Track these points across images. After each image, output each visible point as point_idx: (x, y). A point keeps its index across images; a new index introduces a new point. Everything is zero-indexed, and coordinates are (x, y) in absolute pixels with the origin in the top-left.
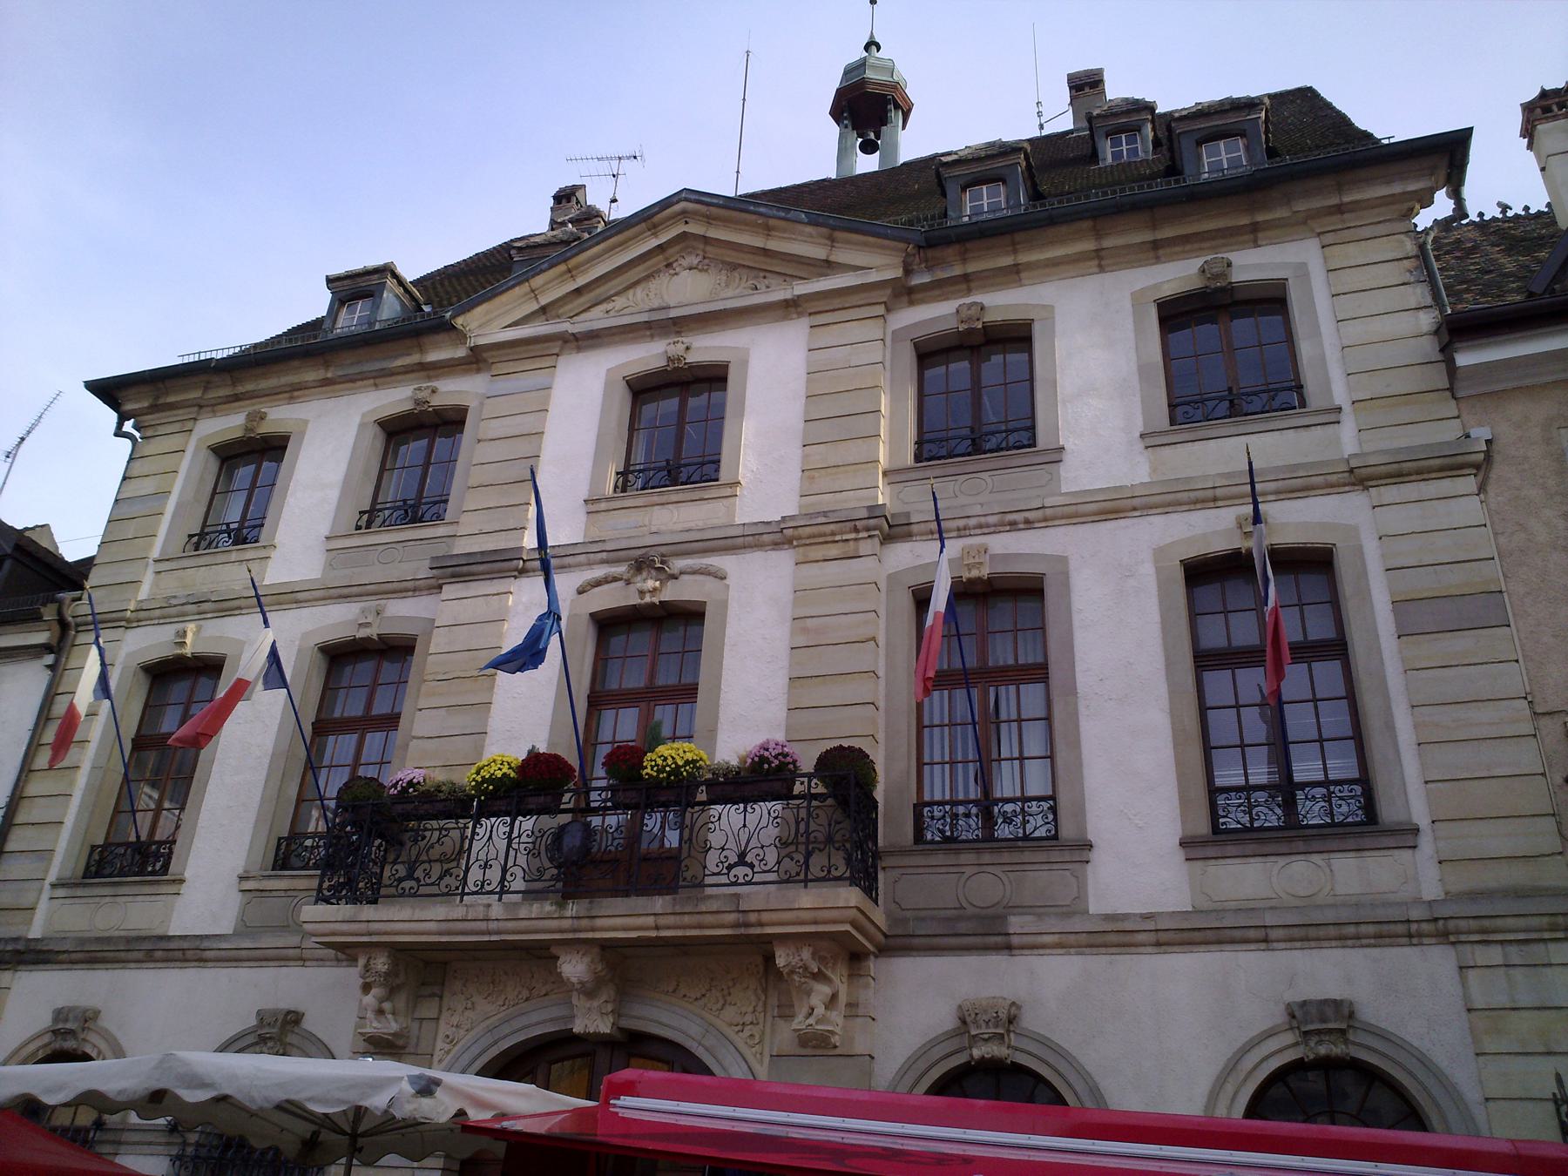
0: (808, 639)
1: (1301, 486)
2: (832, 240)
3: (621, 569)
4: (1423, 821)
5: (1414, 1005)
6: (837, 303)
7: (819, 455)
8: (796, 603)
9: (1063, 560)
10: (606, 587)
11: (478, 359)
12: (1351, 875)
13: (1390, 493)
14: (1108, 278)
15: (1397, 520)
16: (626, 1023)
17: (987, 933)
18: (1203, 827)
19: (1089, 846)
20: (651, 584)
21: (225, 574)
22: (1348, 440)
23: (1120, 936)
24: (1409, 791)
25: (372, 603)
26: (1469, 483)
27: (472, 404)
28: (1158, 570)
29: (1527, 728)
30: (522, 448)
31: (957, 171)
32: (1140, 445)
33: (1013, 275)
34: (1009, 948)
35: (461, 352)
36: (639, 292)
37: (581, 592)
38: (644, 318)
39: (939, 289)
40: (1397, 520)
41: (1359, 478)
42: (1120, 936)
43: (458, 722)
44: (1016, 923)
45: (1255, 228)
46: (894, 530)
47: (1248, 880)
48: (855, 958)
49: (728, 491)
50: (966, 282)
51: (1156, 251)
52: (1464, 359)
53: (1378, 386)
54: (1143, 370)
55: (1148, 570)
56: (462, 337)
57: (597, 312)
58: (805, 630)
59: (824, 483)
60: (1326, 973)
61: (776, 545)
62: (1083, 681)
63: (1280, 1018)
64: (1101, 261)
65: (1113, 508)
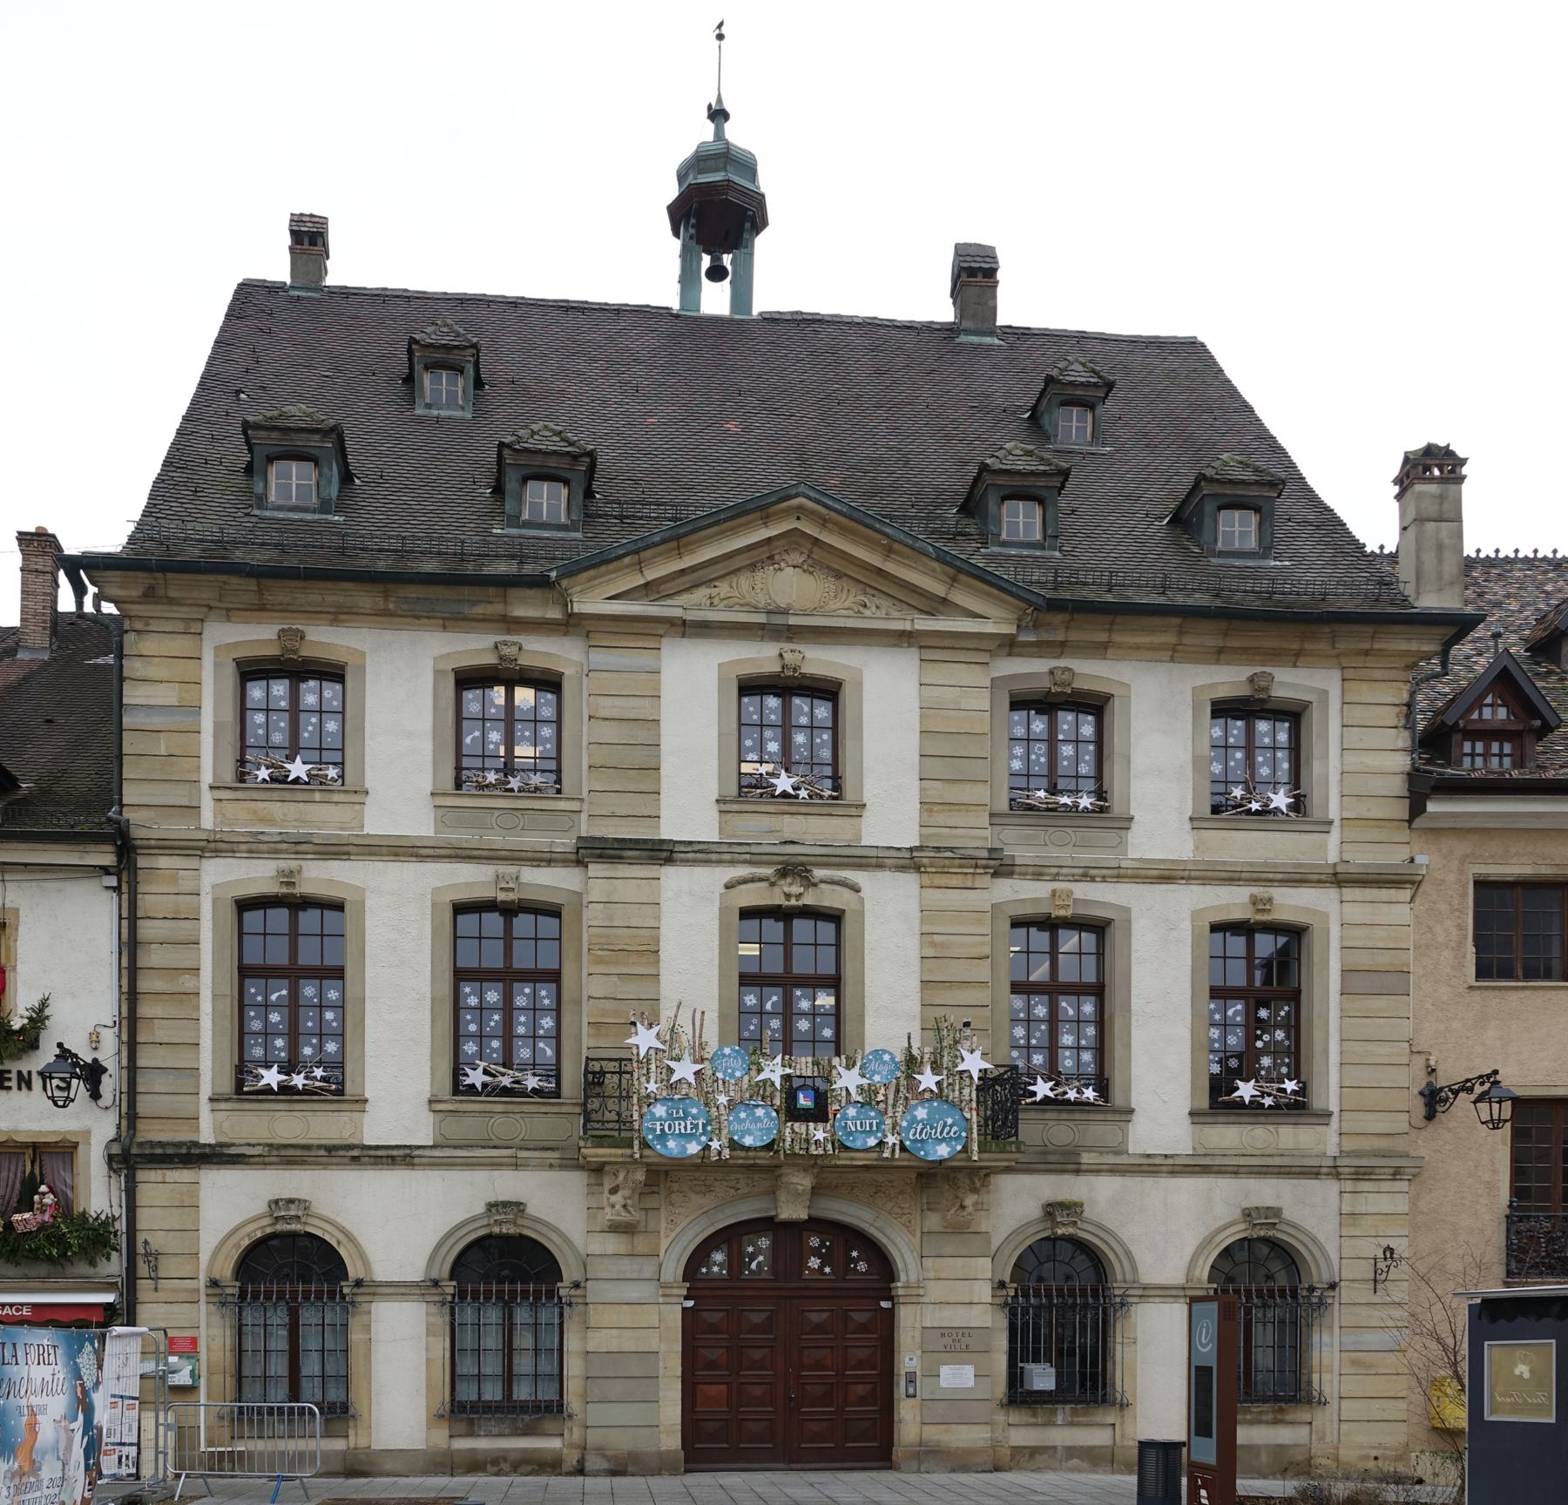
0: (934, 952)
1: (1298, 879)
3: (768, 871)
4: (1334, 1106)
5: (1312, 1213)
11: (572, 624)
12: (1290, 1137)
15: (1355, 913)
17: (1066, 1162)
18: (1204, 1103)
19: (1132, 1111)
22: (1331, 848)
24: (1329, 1091)
25: (511, 869)
26: (1406, 894)
27: (569, 672)
29: (1405, 1060)
30: (641, 735)
32: (1188, 826)
33: (1100, 650)
34: (1077, 1172)
35: (554, 613)
40: (1355, 913)
41: (1338, 879)
43: (629, 990)
44: (1087, 1158)
45: (1298, 654)
46: (1001, 867)
47: (1229, 1136)
49: (853, 811)
50: (1062, 648)
51: (1219, 655)
53: (1363, 809)
55: (1187, 925)
57: (701, 594)
58: (933, 945)
59: (941, 818)
60: (1265, 1192)
61: (901, 868)
62: (1136, 1003)
63: (1237, 1214)
64: (1175, 654)
65: (1167, 875)
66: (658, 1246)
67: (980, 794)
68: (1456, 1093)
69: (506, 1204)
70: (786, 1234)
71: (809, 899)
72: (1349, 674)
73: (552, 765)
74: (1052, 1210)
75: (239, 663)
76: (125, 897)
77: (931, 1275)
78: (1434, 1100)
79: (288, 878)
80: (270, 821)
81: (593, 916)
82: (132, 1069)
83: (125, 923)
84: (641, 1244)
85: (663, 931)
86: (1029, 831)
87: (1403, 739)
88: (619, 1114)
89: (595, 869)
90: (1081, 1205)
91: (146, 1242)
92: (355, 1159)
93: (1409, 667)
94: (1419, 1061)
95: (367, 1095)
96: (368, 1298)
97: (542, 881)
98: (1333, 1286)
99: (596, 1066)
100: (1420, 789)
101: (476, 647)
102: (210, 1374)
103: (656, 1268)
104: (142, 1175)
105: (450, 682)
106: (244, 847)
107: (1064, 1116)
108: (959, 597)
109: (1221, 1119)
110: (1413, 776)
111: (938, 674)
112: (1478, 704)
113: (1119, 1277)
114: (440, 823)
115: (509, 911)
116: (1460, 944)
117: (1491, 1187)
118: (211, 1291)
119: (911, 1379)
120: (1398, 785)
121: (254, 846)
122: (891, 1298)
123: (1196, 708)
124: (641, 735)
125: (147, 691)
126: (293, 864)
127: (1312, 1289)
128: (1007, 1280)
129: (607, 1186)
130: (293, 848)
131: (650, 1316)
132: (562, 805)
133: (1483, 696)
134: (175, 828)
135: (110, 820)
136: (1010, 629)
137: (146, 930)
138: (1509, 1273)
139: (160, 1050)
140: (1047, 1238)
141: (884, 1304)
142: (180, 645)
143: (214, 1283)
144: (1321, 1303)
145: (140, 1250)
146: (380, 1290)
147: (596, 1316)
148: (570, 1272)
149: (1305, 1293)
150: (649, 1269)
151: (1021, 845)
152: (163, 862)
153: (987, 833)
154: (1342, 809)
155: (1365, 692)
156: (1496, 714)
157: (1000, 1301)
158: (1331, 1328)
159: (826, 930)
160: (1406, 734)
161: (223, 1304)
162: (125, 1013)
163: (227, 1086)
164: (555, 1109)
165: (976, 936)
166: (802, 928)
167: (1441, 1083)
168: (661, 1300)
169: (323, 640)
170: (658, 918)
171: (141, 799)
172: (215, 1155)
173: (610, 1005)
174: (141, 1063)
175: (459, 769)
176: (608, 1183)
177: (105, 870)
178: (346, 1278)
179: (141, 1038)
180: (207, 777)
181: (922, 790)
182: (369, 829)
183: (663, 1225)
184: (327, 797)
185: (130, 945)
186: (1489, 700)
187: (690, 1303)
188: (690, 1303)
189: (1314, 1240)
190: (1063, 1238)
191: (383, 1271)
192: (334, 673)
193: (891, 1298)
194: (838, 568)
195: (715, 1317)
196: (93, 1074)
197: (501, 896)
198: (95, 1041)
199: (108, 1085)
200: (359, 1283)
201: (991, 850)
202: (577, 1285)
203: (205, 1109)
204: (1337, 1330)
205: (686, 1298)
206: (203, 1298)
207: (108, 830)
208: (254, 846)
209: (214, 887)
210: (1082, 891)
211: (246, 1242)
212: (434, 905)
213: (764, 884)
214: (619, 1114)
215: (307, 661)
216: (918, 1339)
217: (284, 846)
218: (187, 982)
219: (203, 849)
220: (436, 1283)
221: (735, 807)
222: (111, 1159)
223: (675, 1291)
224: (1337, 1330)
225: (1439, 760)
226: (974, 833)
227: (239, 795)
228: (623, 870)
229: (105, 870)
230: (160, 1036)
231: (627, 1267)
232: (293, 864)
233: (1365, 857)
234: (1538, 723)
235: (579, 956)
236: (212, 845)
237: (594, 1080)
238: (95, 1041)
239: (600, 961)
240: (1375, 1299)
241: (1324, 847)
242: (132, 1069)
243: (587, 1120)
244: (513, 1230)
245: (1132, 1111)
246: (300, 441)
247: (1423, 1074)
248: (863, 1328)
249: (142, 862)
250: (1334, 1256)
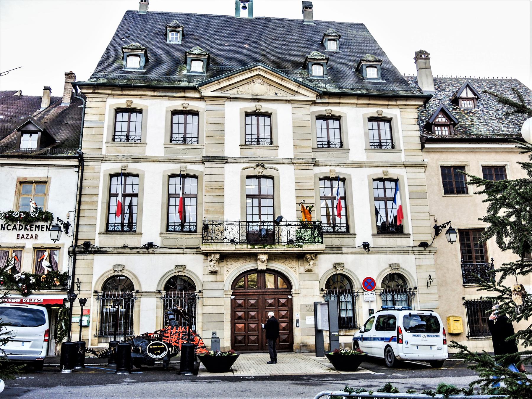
2: (299, 87)
3: (254, 165)
4: (411, 233)
6: (299, 103)
7: (299, 143)
8: (296, 179)
11: (202, 98)
15: (411, 176)
16: (268, 267)
17: (338, 250)
19: (356, 234)
20: (261, 170)
22: (402, 158)
26: (423, 170)
28: (368, 180)
29: (428, 218)
30: (219, 128)
31: (312, 61)
32: (365, 151)
35: (197, 95)
36: (246, 86)
38: (251, 97)
40: (411, 176)
48: (316, 254)
49: (276, 148)
52: (427, 146)
53: (409, 147)
55: (366, 179)
56: (199, 92)
58: (298, 186)
59: (299, 150)
66: (224, 278)
67: (309, 143)
68: (442, 227)
69: (181, 266)
70: (262, 273)
71: (265, 173)
72: (402, 110)
73: (196, 136)
74: (336, 266)
75: (116, 109)
76: (80, 174)
77: (302, 287)
78: (437, 230)
79: (124, 168)
80: (120, 152)
81: (206, 178)
82: (78, 225)
83: (79, 181)
84: (218, 277)
85: (225, 182)
86: (323, 153)
87: (417, 127)
88: (212, 238)
89: (207, 165)
90: (343, 264)
91: (78, 279)
92: (138, 252)
93: (418, 108)
94: (432, 218)
95: (142, 232)
96: (140, 296)
97: (192, 168)
98: (416, 288)
99: (206, 223)
100: (424, 141)
101: (177, 104)
102: (93, 321)
103: (223, 286)
104: (78, 257)
105: (170, 114)
106: (113, 159)
107: (337, 236)
108: (301, 90)
109: (380, 236)
110: (421, 137)
111: (297, 111)
112: (437, 117)
113: (356, 287)
114: (166, 152)
115: (184, 177)
116: (439, 184)
117: (456, 255)
118: (95, 294)
119: (298, 321)
120: (418, 140)
121: (116, 159)
122: (291, 295)
123: (364, 119)
124: (219, 128)
125: (90, 118)
126: (126, 164)
127: (410, 289)
128: (324, 288)
129: (209, 259)
130: (126, 159)
131: (221, 302)
132: (198, 147)
133: (438, 115)
135: (78, 152)
136: (314, 99)
137: (85, 183)
138: (464, 283)
139: (86, 219)
140: (335, 275)
141: (290, 297)
142: (101, 104)
143: (96, 292)
144: (413, 294)
145: (76, 281)
146: (143, 294)
147: (207, 301)
148: (198, 288)
149: (408, 290)
150: (221, 286)
151: (321, 157)
152: (91, 164)
153: (312, 154)
154: (404, 146)
155: (406, 115)
156: (441, 119)
157: (322, 295)
158: (417, 301)
159: (270, 182)
160: (418, 126)
161: (98, 298)
162: (77, 208)
163: (103, 230)
164: (195, 236)
165: (310, 183)
166: (263, 181)
167: (438, 225)
168: (225, 296)
169: (137, 103)
170: (224, 179)
171: (87, 147)
172: (99, 251)
173: (210, 204)
174: (80, 223)
175: (171, 137)
176: (209, 259)
177: (76, 166)
178: (134, 290)
179: (81, 215)
181: (294, 142)
182: (147, 154)
183: (225, 272)
184: (136, 145)
185: (81, 188)
186: (440, 116)
187: (233, 297)
188: (233, 297)
189: (409, 273)
190: (339, 274)
191: (145, 288)
192: (140, 111)
193: (291, 295)
194: (271, 83)
195: (240, 302)
196: (67, 226)
197: (182, 173)
198: (68, 216)
199: (72, 229)
200: (137, 292)
201: (312, 159)
202: (200, 292)
203: (97, 236)
204: (419, 302)
205: (232, 295)
206: (92, 297)
207: (77, 155)
208: (116, 159)
209: (104, 171)
210: (338, 170)
211: (106, 278)
212: (163, 175)
213: (253, 169)
214: (212, 238)
215: (133, 109)
216: (299, 308)
217: (124, 159)
218: (94, 199)
219: (102, 160)
220: (159, 292)
221: (244, 147)
222: (69, 252)
223: (229, 293)
224: (419, 302)
225: (428, 134)
226: (308, 154)
227: (113, 145)
228: (214, 165)
229: (76, 166)
230: (86, 215)
231: (215, 286)
232: (126, 164)
233: (412, 160)
234: (453, 122)
235: (202, 190)
236: (104, 159)
237: (206, 228)
238: (68, 216)
239: (208, 191)
240: (428, 292)
241: (400, 157)
242: (78, 225)
243: (203, 239)
244: (182, 274)
245: (356, 234)
246: (136, 52)
247: (434, 222)
248: (283, 305)
249: (85, 164)
250: (416, 279)
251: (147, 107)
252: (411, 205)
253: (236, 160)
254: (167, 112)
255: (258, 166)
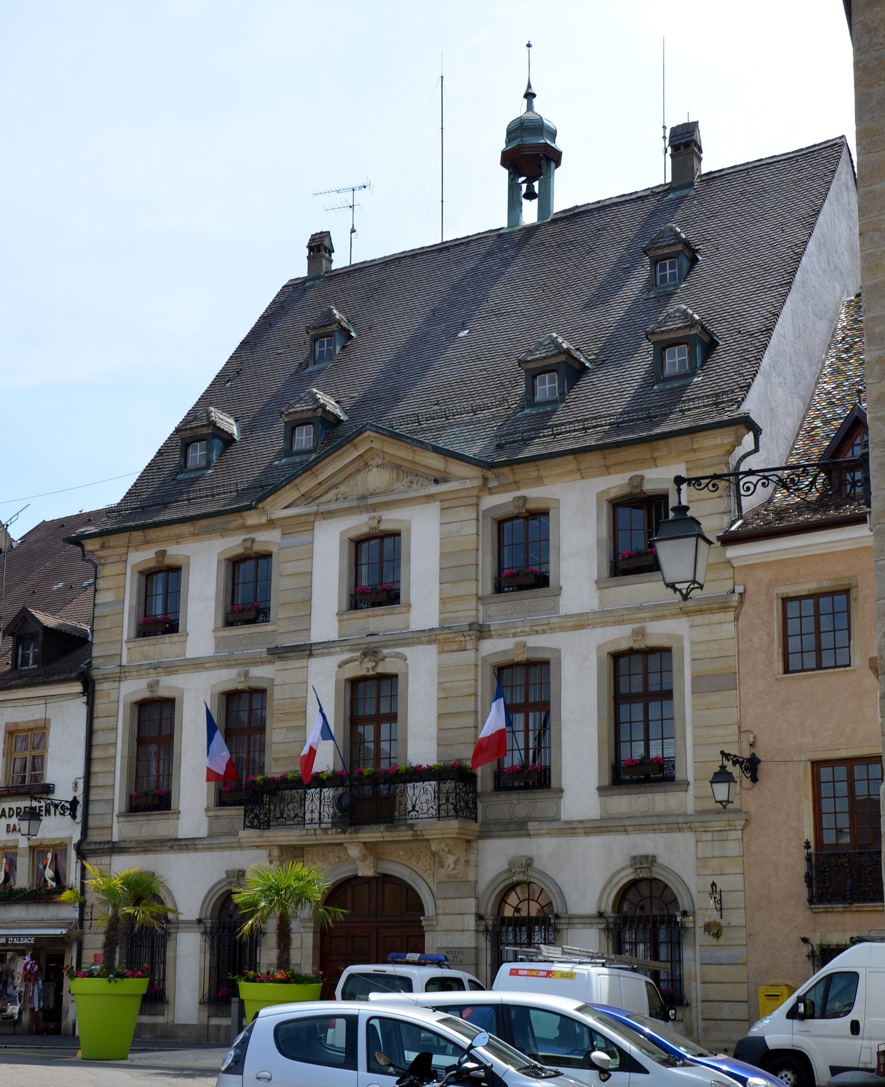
0: (445, 694)
1: (659, 612)
4: (691, 778)
8: (440, 674)
9: (558, 651)
10: (351, 664)
12: (660, 801)
13: (698, 619)
14: (586, 482)
18: (607, 781)
21: (162, 647)
23: (573, 829)
27: (274, 550)
28: (598, 657)
33: (539, 481)
34: (529, 835)
37: (340, 666)
39: (504, 488)
42: (573, 829)
50: (517, 485)
51: (607, 470)
54: (599, 541)
58: (443, 689)
60: (648, 843)
65: (581, 622)
74: (512, 864)
134: (110, 668)
139: (99, 791)
174: (92, 797)
180: (125, 638)
185: (90, 732)
203: (115, 819)
249: (98, 687)
251: (189, 557)
252: (695, 708)
253: (327, 647)
254: (219, 561)
255: (365, 654)
